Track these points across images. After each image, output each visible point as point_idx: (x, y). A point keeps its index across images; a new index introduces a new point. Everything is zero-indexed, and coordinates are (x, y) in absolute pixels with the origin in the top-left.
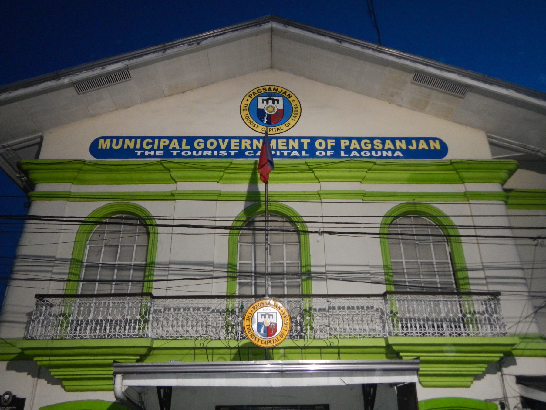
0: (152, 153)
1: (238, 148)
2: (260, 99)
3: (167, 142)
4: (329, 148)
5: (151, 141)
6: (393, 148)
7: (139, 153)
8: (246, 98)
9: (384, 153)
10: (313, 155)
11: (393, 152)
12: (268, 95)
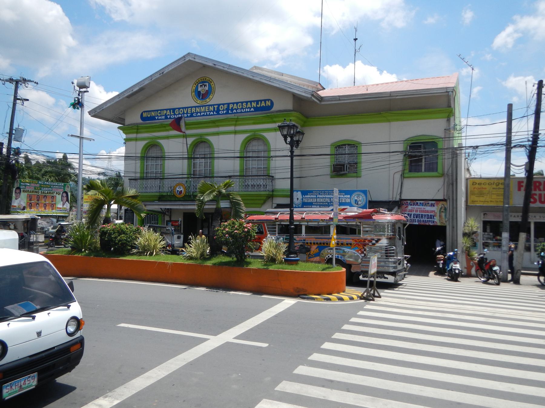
0: (161, 118)
1: (191, 112)
2: (199, 85)
3: (166, 111)
4: (225, 109)
5: (160, 112)
6: (250, 107)
7: (157, 118)
8: (194, 86)
9: (247, 109)
10: (218, 114)
11: (250, 109)
12: (202, 82)
